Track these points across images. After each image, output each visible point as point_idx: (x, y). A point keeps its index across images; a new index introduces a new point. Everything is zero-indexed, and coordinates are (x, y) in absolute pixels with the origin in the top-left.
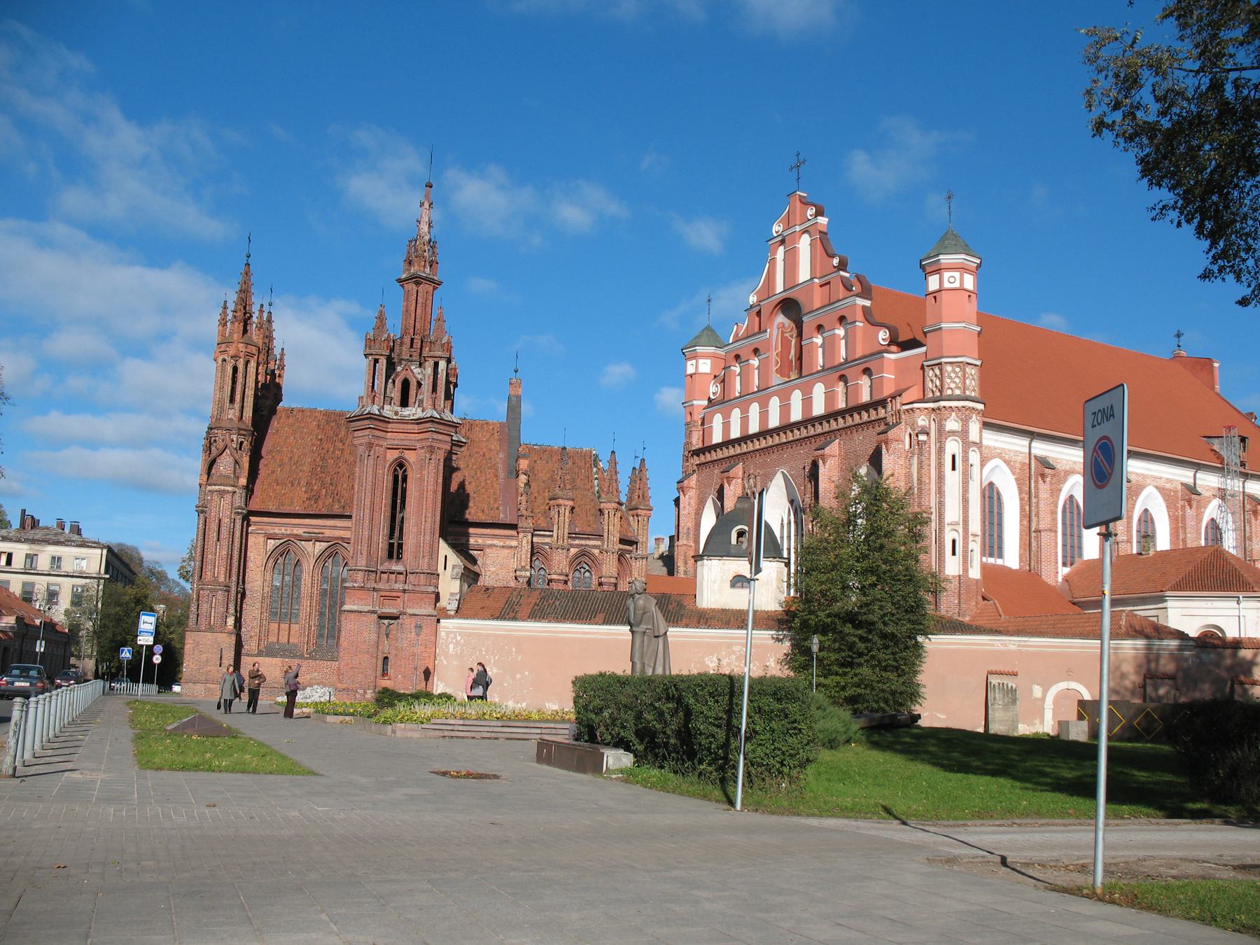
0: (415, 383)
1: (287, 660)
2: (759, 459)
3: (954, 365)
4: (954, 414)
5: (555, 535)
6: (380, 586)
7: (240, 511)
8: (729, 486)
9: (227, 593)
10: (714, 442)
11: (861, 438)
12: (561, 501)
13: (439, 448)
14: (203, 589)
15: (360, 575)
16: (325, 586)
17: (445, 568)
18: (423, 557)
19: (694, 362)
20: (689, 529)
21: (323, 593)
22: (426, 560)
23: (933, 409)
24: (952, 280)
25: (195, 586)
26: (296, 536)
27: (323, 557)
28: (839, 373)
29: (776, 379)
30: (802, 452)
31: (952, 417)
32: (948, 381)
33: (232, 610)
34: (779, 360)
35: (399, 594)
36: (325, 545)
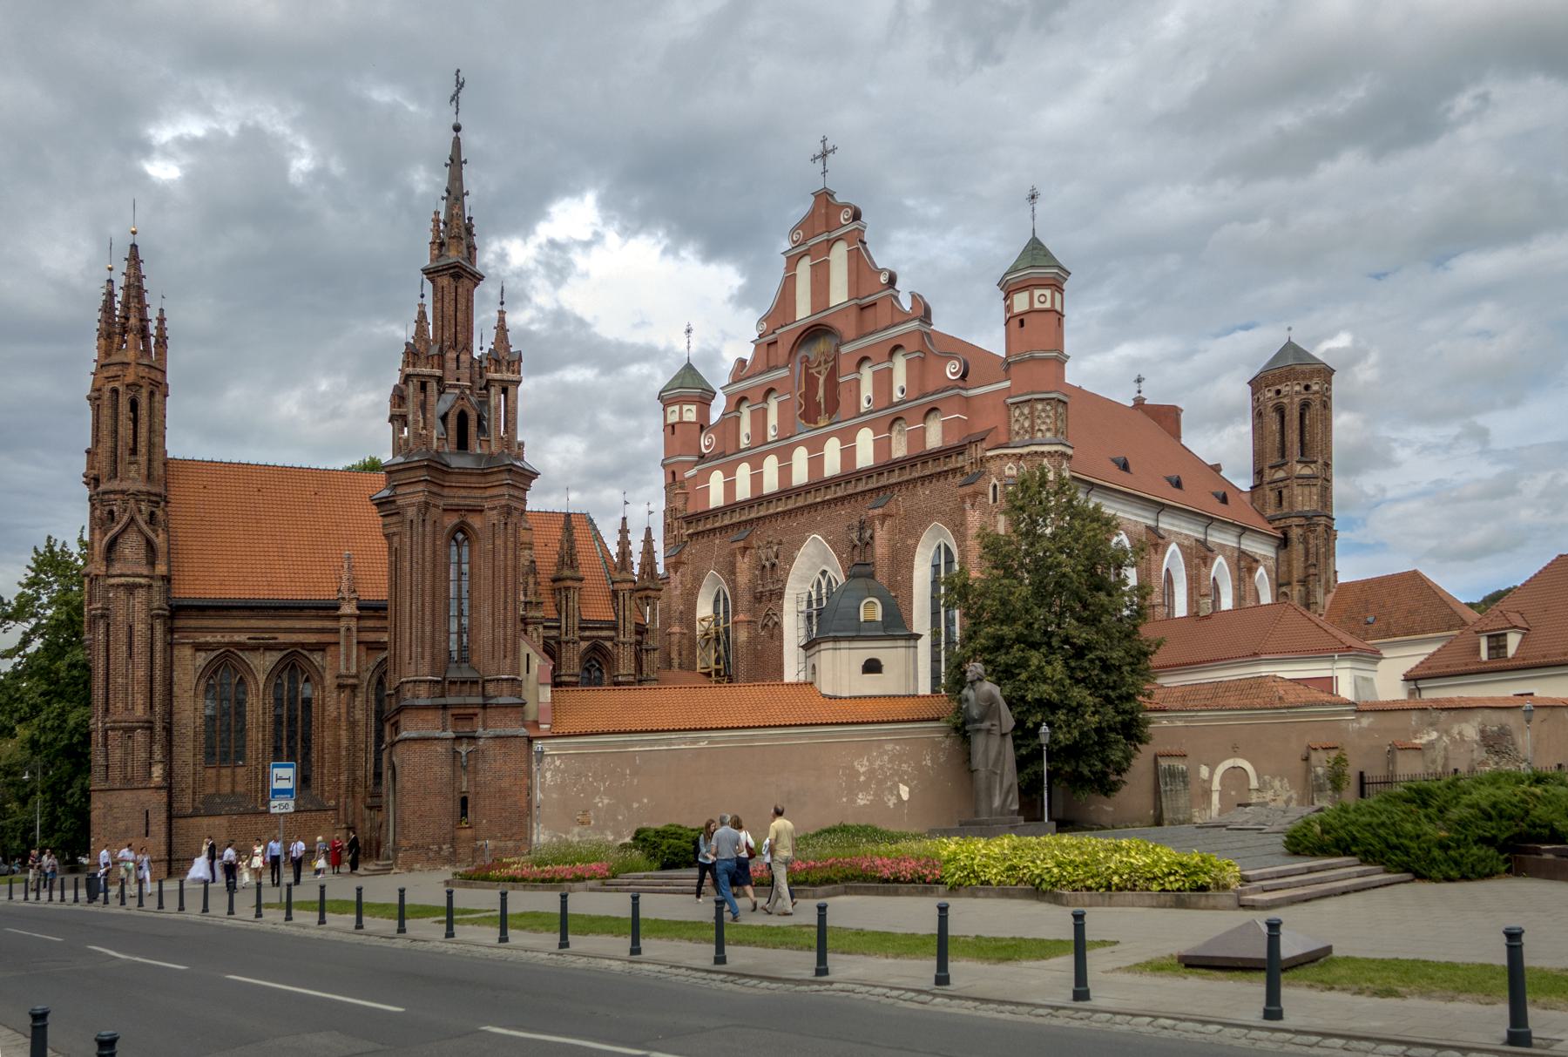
1: (235, 817)
2: (781, 524)
5: (564, 626)
7: (160, 612)
8: (743, 557)
9: (149, 732)
10: (711, 507)
11: (927, 492)
12: (569, 583)
14: (113, 729)
15: (423, 690)
16: (279, 711)
17: (528, 672)
18: (505, 657)
21: (278, 720)
22: (508, 661)
23: (1022, 455)
25: (100, 725)
26: (242, 646)
27: (275, 673)
28: (890, 418)
32: (1039, 421)
33: (158, 756)
36: (277, 656)
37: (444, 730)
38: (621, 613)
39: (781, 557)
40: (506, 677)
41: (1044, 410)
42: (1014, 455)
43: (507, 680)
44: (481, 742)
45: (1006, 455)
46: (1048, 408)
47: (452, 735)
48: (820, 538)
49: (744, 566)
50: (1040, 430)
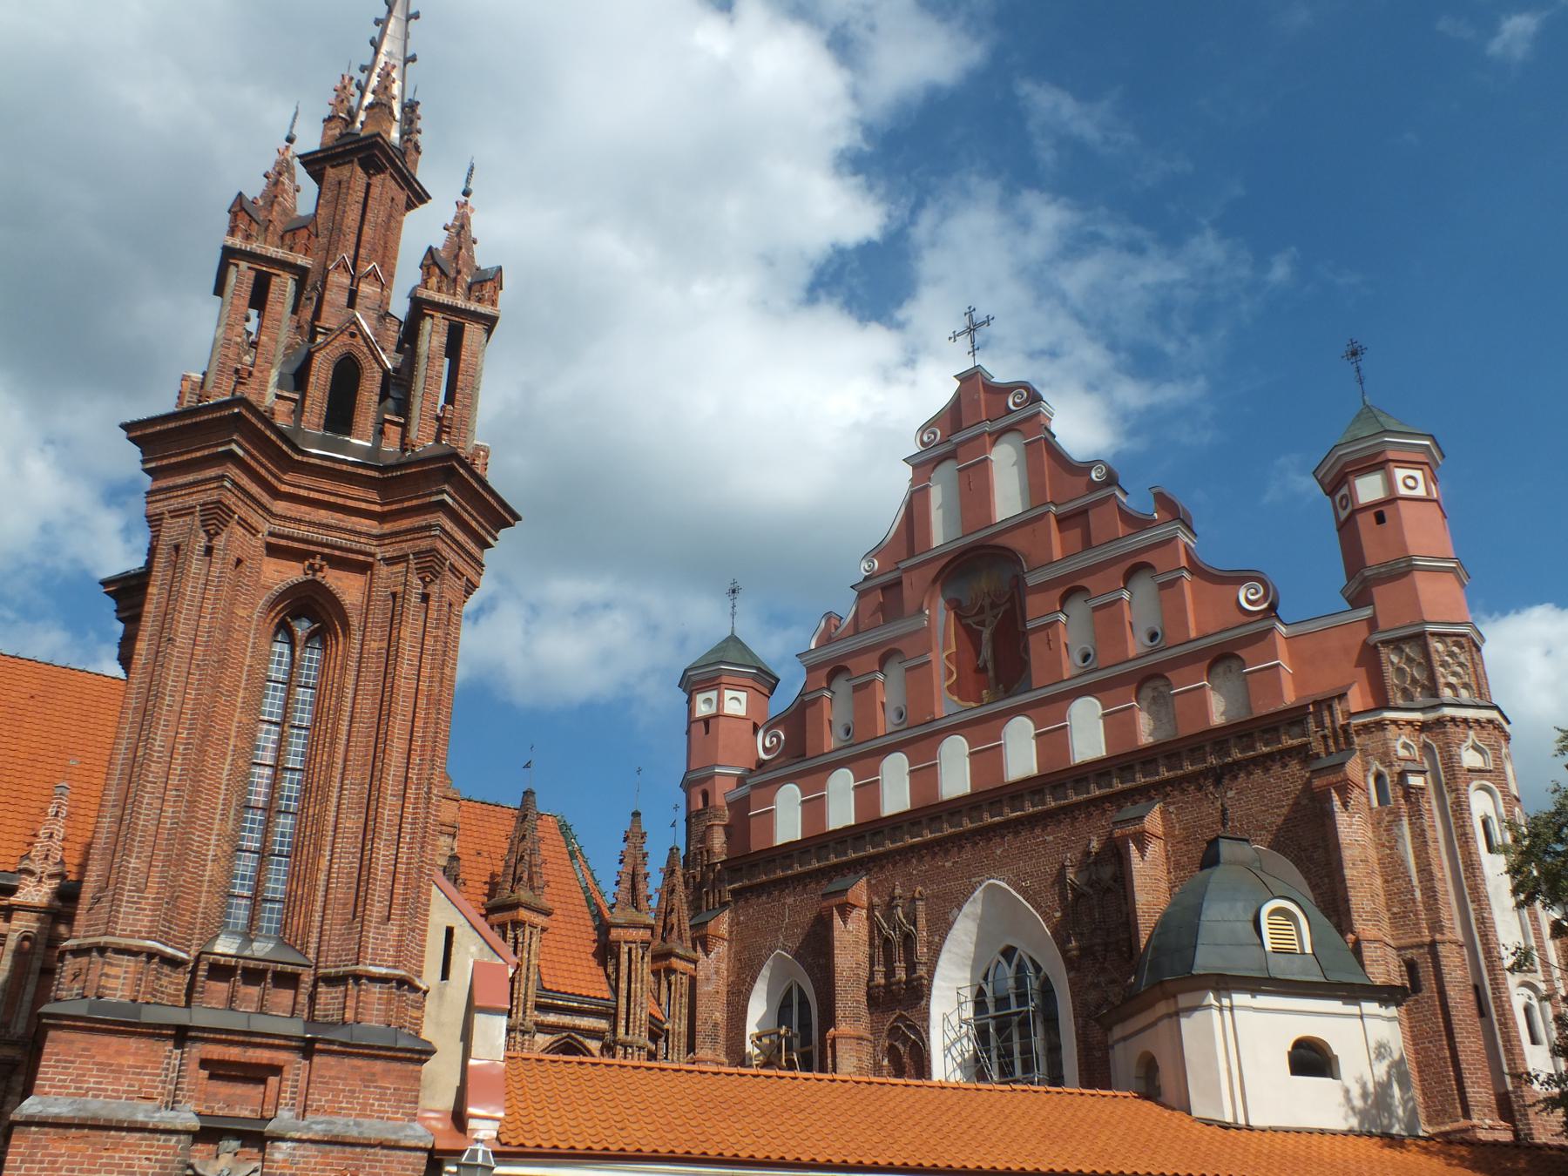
0: (378, 377)
2: (916, 868)
3: (1449, 640)
4: (1471, 733)
6: (199, 1017)
8: (845, 922)
10: (779, 842)
12: (523, 914)
13: (453, 568)
17: (445, 975)
19: (713, 695)
20: (716, 1025)
22: (393, 929)
24: (1411, 483)
29: (946, 705)
30: (1051, 838)
31: (1470, 742)
34: (953, 669)
35: (280, 1057)
37: (173, 1104)
38: (623, 985)
39: (922, 922)
40: (384, 971)
41: (1452, 654)
42: (1409, 723)
43: (383, 980)
44: (279, 1153)
45: (1394, 722)
46: (1456, 649)
47: (187, 1118)
48: (1004, 885)
49: (848, 937)
50: (1450, 685)
